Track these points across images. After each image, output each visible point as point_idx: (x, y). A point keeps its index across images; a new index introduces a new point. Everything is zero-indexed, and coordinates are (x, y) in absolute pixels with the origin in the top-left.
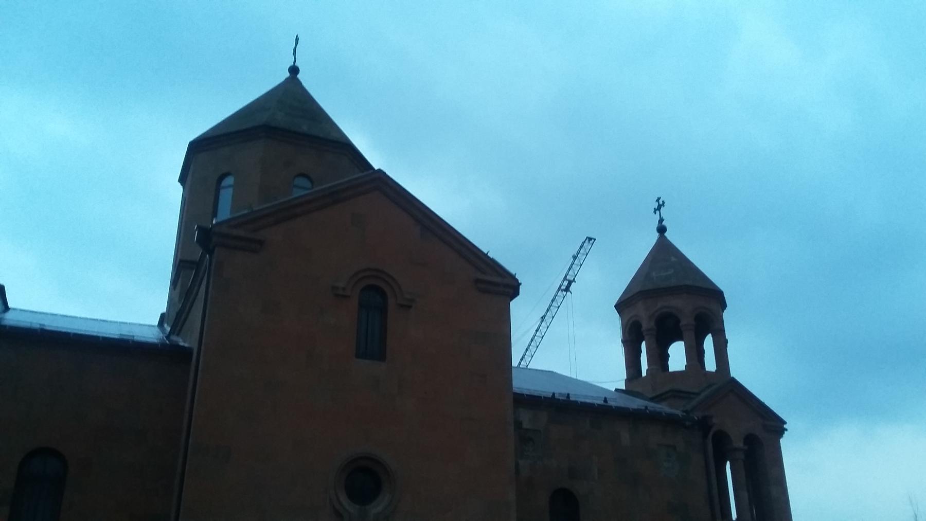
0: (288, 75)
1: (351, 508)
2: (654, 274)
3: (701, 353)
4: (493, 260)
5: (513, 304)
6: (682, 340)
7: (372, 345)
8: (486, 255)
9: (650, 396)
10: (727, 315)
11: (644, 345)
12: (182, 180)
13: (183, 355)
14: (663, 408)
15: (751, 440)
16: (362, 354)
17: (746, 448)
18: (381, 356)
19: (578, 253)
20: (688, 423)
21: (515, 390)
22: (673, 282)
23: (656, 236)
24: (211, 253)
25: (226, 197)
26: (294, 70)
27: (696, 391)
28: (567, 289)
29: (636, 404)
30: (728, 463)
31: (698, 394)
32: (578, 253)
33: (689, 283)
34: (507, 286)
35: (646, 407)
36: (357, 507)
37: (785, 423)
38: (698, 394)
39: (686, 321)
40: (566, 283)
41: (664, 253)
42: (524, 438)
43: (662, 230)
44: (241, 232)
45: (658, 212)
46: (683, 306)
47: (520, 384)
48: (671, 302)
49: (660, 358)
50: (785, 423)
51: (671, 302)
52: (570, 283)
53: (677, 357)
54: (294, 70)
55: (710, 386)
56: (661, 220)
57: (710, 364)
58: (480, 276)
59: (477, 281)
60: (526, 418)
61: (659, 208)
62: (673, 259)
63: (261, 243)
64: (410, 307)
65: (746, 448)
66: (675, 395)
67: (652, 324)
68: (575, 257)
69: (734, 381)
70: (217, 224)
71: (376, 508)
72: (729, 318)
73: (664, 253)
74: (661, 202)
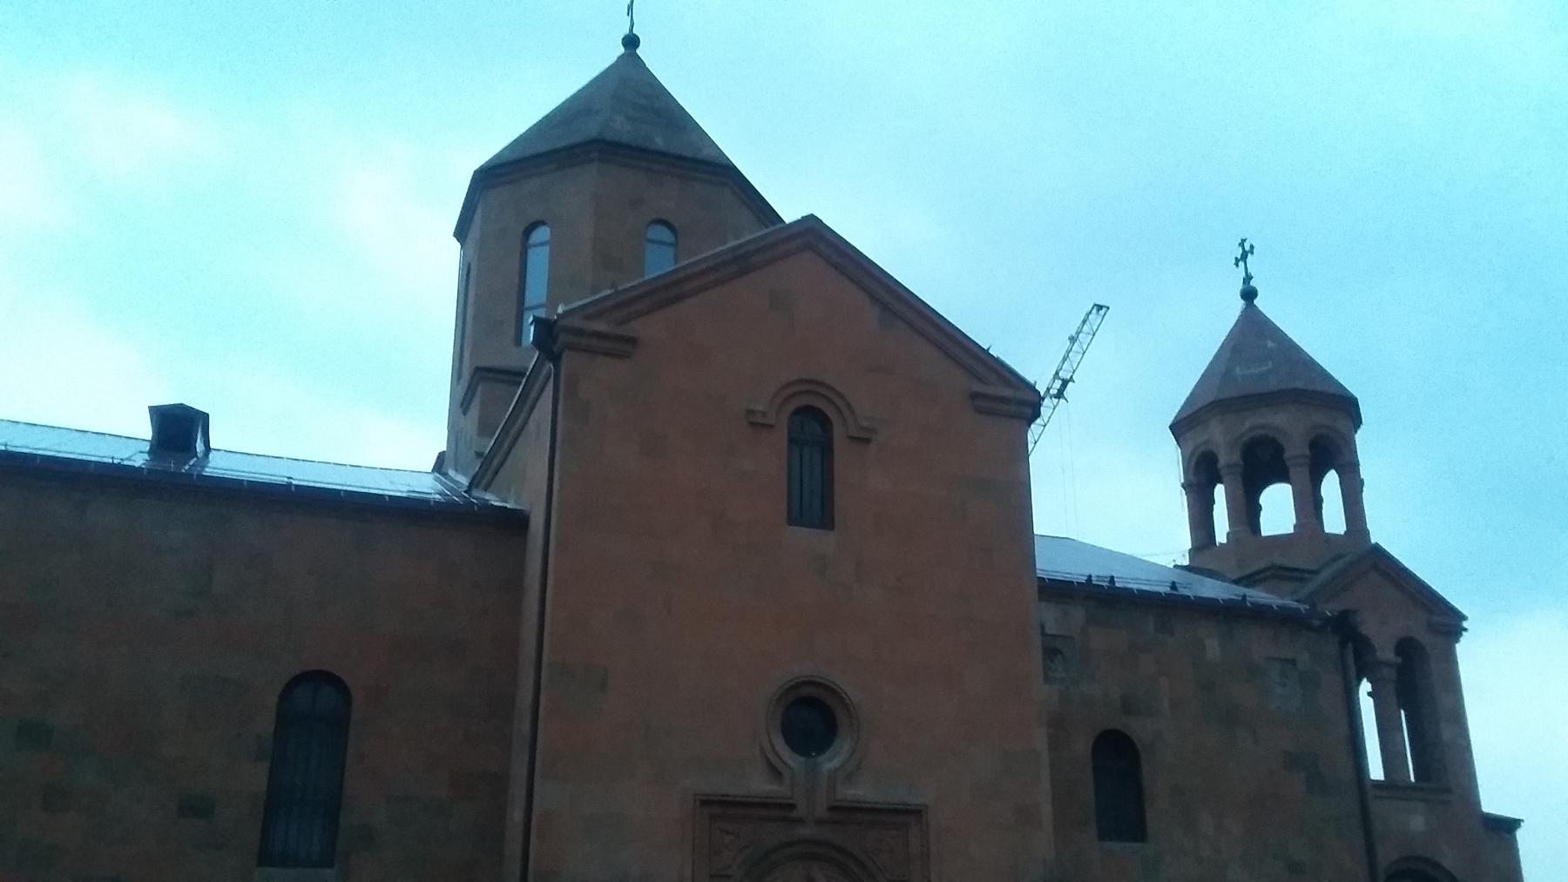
0: (622, 50)
1: (792, 760)
2: (1238, 371)
3: (1317, 502)
4: (997, 360)
5: (1035, 428)
6: (1283, 477)
7: (814, 505)
8: (986, 352)
9: (1235, 577)
10: (1361, 438)
11: (1220, 491)
12: (461, 233)
13: (515, 522)
14: (1258, 595)
16: (797, 517)
17: (1399, 660)
18: (825, 521)
19: (1078, 333)
20: (1316, 623)
21: (1040, 574)
22: (1273, 384)
23: (1241, 304)
24: (556, 359)
25: (539, 262)
26: (631, 42)
27: (1315, 567)
28: (1060, 395)
29: (1211, 589)
30: (1365, 687)
32: (1078, 333)
33: (1299, 385)
34: (1023, 403)
35: (1244, 597)
36: (802, 759)
37: (1464, 618)
40: (1058, 384)
41: (1254, 334)
43: (1249, 295)
44: (601, 326)
45: (1241, 264)
47: (1048, 564)
48: (1267, 417)
49: (1246, 513)
50: (1464, 618)
51: (1267, 417)
52: (1065, 383)
53: (1278, 509)
54: (631, 42)
55: (1339, 557)
56: (1248, 278)
58: (978, 387)
59: (975, 396)
60: (1051, 616)
61: (1244, 256)
62: (1270, 344)
63: (633, 341)
64: (868, 441)
65: (1399, 660)
67: (1236, 457)
68: (1073, 340)
69: (1378, 551)
70: (566, 314)
71: (830, 762)
73: (1254, 334)
74: (1247, 248)
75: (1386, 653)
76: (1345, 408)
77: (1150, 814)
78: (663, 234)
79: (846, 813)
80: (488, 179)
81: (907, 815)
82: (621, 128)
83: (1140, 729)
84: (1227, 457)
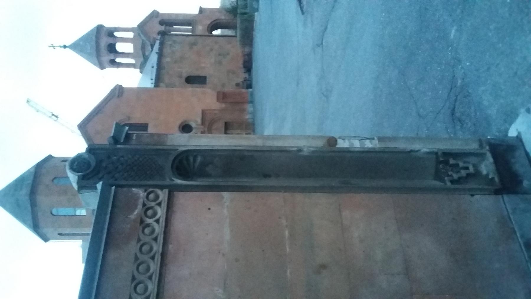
1: (194, 131)
2: (89, 51)
11: (118, 60)
12: (46, 240)
15: (162, 23)
22: (93, 43)
23: (67, 49)
27: (141, 41)
31: (143, 41)
33: (94, 38)
38: (143, 41)
39: (111, 40)
41: (77, 47)
42: (171, 85)
43: (65, 47)
46: (104, 41)
56: (60, 47)
57: (130, 35)
58: (117, 95)
59: (118, 97)
61: (53, 46)
66: (143, 48)
69: (139, 26)
71: (193, 125)
72: (108, 24)
73: (77, 47)
75: (162, 28)
76: (99, 28)
77: (201, 75)
78: (56, 181)
79: (203, 123)
80: (36, 228)
81: (204, 113)
82: (25, 191)
83: (185, 75)
84: (112, 57)
